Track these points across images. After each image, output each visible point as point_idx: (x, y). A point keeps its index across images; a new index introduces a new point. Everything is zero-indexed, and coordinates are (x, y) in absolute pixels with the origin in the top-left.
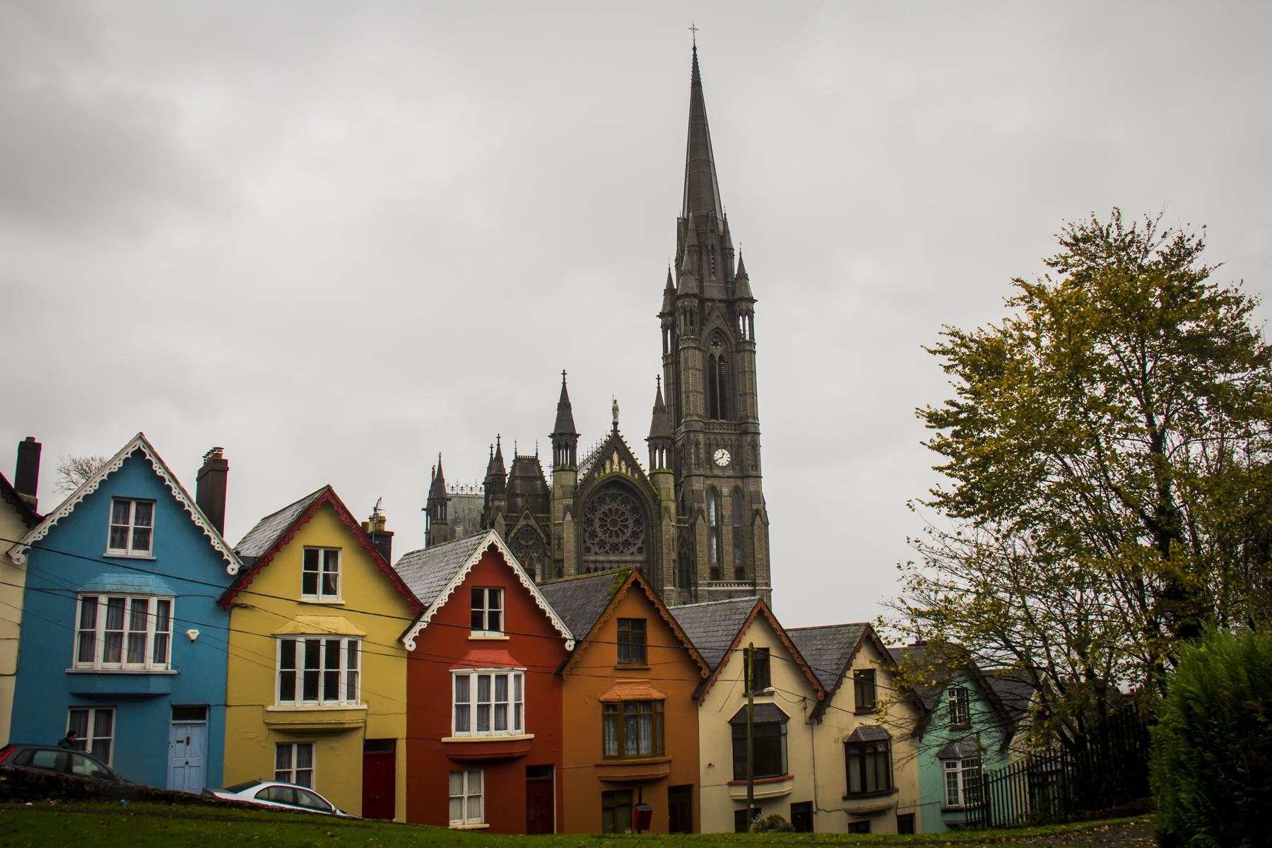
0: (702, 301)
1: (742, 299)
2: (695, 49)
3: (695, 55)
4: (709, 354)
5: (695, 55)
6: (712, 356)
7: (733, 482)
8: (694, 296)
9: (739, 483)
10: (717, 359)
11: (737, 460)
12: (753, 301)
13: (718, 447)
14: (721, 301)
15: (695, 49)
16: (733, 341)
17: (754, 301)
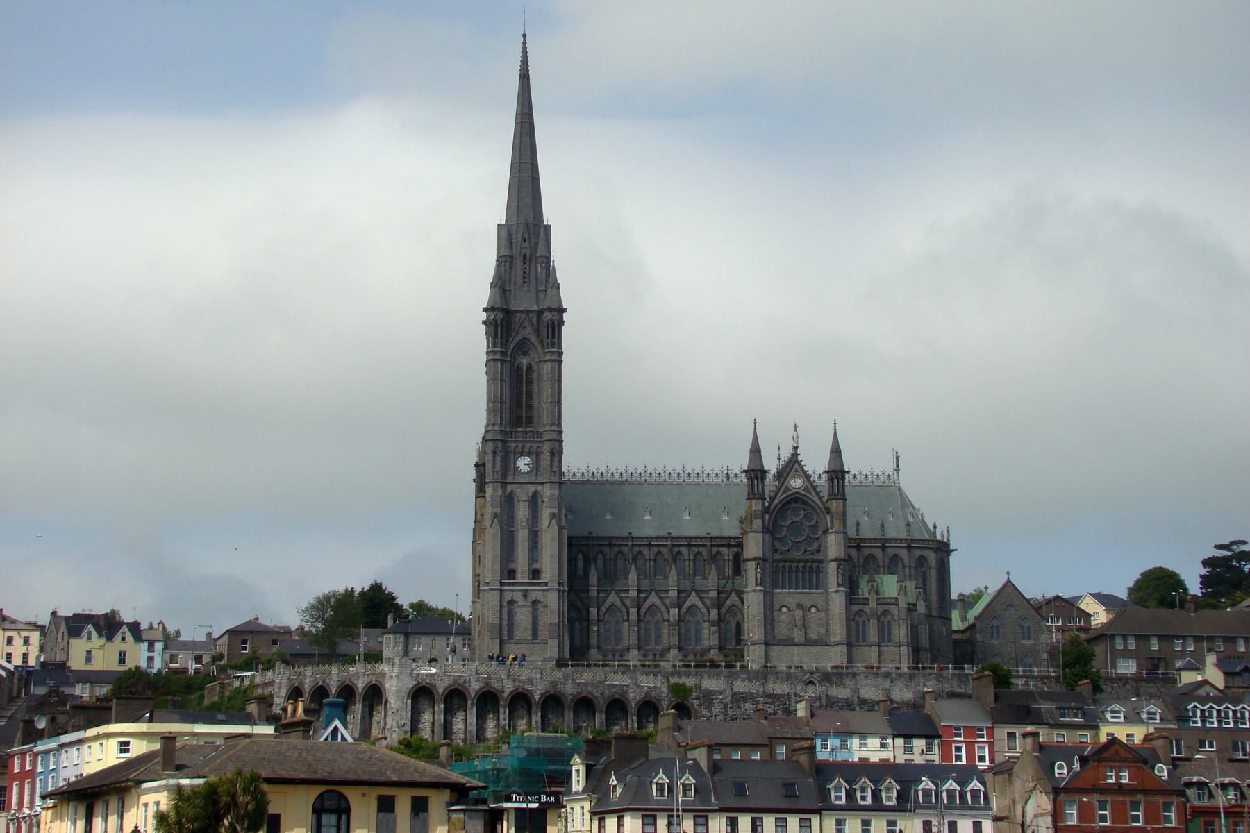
0: (508, 313)
1: (550, 309)
2: (524, 36)
3: (524, 43)
4: (517, 364)
5: (524, 43)
6: (519, 368)
7: (532, 489)
8: (502, 310)
9: (539, 488)
10: (525, 369)
11: (536, 466)
12: (564, 310)
13: (522, 454)
14: (528, 312)
15: (524, 36)
16: (540, 350)
17: (564, 310)
